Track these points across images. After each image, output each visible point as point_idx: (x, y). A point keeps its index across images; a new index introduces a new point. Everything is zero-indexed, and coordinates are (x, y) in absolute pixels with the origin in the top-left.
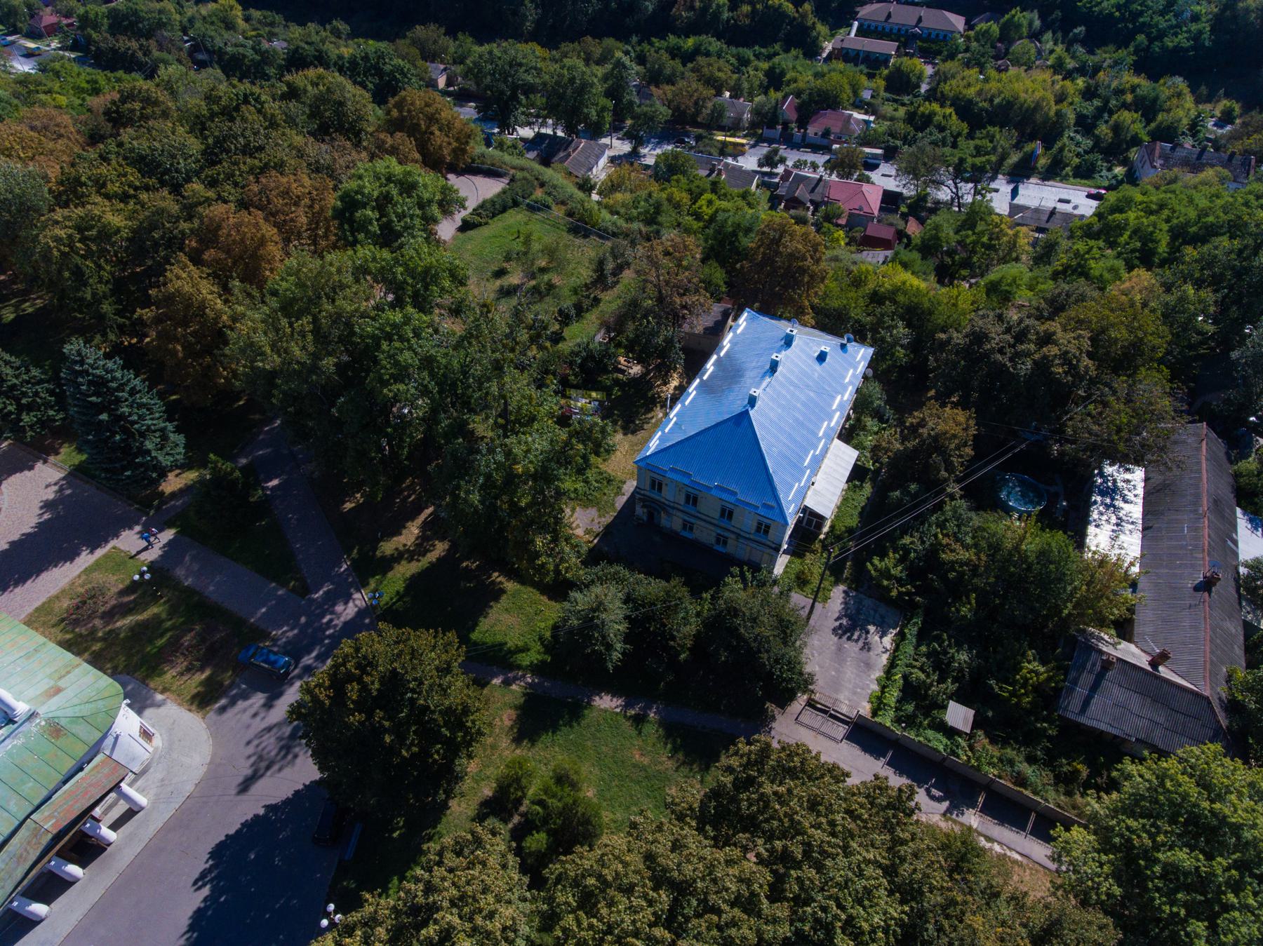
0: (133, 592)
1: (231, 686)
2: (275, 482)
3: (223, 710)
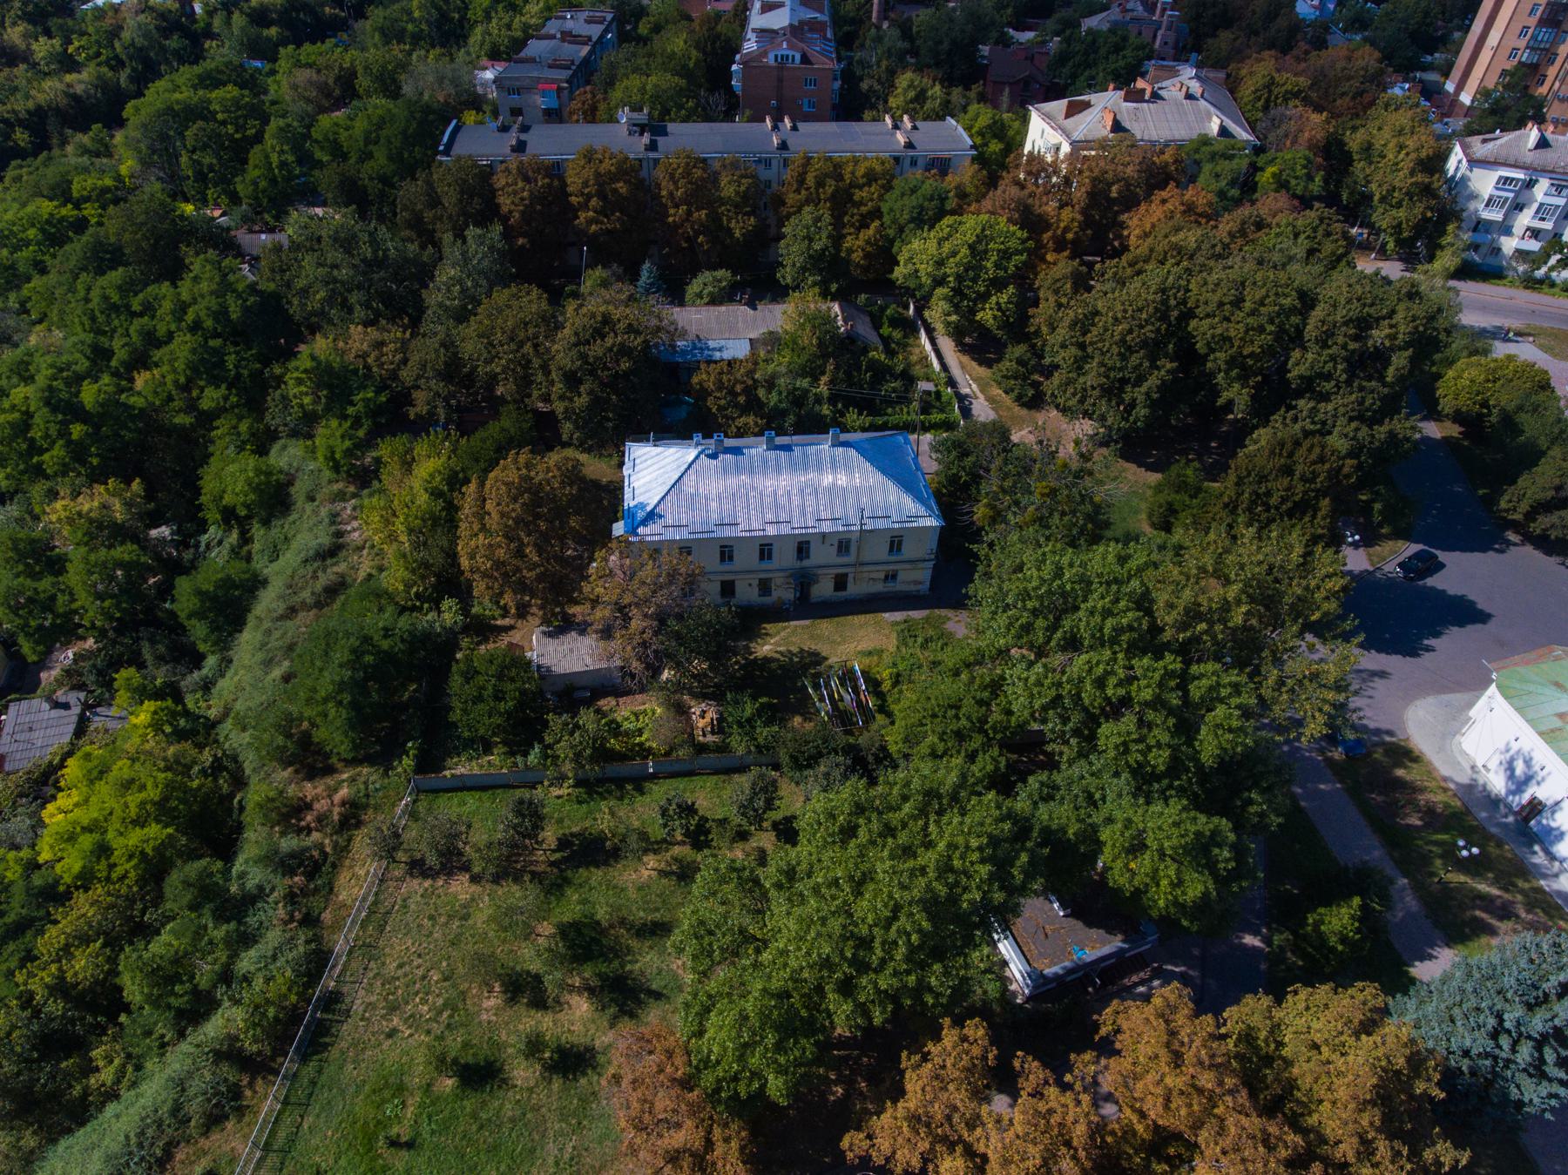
0: (1475, 919)
1: (1376, 745)
2: (1250, 940)
3: (1390, 733)
